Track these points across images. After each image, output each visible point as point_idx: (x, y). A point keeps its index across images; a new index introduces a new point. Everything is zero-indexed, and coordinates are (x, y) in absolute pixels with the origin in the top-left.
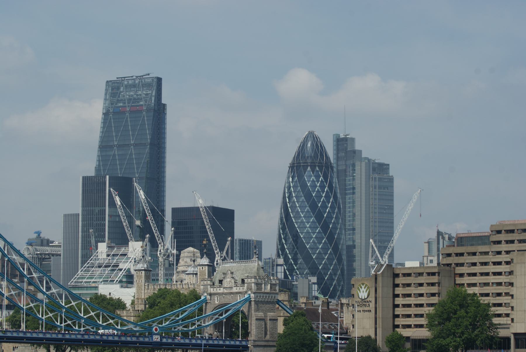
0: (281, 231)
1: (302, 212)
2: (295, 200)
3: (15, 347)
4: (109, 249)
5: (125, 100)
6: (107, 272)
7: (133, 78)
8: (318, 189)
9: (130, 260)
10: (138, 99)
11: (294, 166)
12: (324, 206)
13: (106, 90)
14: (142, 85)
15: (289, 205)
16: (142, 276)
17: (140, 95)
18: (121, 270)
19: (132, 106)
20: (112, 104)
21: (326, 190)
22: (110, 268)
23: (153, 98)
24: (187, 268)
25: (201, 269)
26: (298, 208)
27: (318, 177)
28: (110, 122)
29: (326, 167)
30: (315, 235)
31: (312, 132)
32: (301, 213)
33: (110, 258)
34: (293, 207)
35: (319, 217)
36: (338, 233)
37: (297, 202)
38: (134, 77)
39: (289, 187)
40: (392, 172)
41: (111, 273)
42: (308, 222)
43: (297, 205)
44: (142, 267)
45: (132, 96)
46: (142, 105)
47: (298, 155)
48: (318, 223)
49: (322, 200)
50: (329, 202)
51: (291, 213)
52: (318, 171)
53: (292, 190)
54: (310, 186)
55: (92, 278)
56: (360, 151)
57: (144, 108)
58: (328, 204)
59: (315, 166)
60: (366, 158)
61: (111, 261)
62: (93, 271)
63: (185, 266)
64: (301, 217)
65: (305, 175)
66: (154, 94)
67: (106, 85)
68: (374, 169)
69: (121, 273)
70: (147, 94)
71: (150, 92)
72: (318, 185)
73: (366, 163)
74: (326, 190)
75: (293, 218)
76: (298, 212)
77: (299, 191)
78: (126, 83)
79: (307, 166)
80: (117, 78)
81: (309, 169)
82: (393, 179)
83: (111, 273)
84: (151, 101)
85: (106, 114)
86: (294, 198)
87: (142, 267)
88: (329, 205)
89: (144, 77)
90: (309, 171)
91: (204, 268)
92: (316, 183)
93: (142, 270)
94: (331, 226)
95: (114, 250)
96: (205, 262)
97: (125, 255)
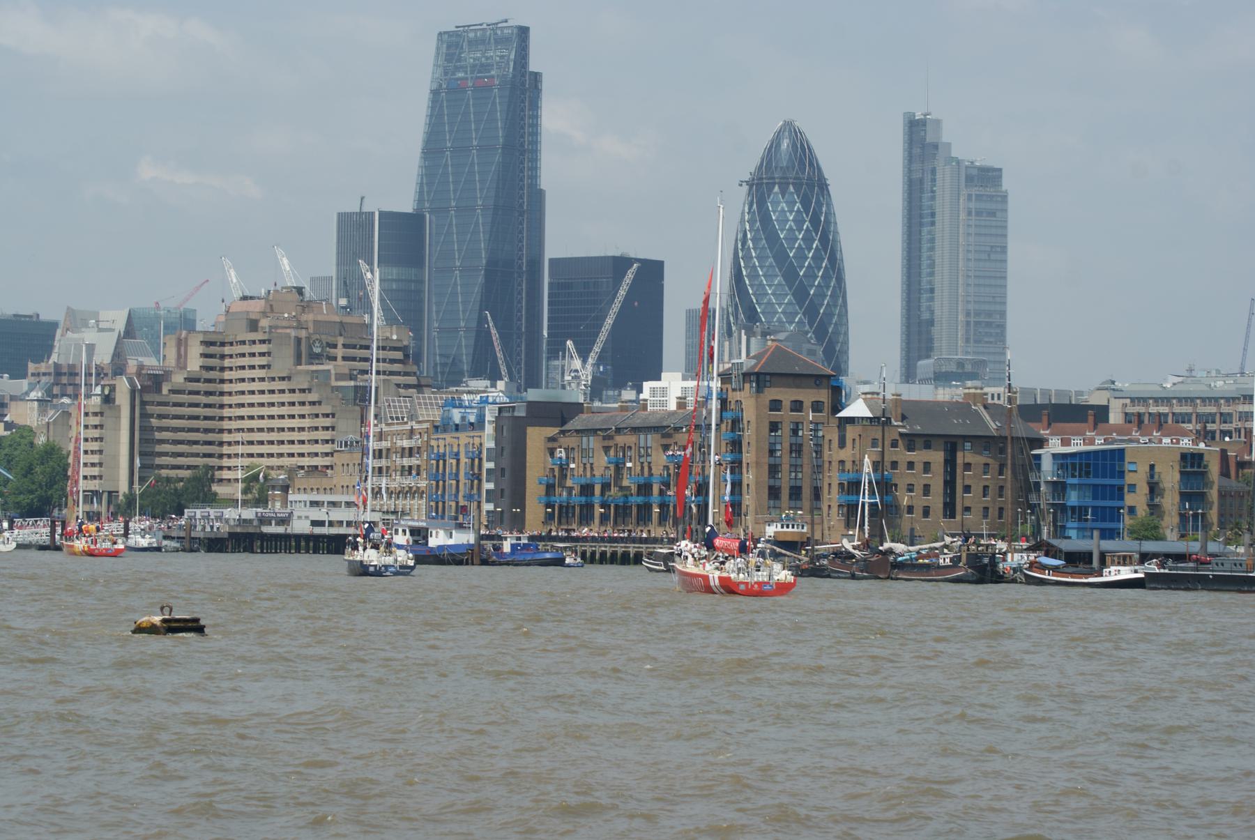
0: (732, 319)
1: (770, 286)
2: (757, 264)
8: (800, 244)
12: (811, 275)
15: (744, 273)
21: (814, 246)
32: (767, 288)
34: (754, 276)
35: (800, 294)
37: (761, 267)
43: (761, 273)
49: (806, 264)
50: (819, 268)
53: (751, 245)
71: (505, 53)
72: (801, 236)
76: (761, 285)
77: (763, 248)
86: (755, 260)
88: (820, 274)
89: (500, 25)
92: (797, 233)
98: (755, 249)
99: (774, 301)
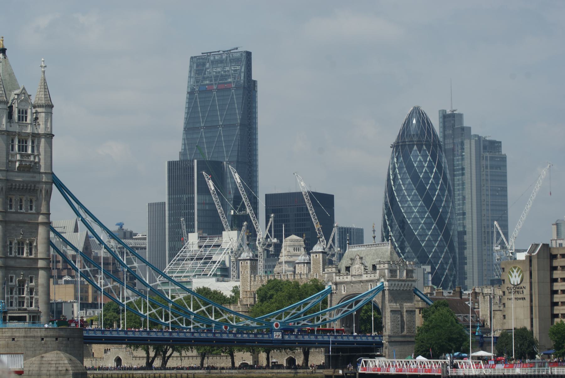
0: (386, 217)
1: (409, 196)
2: (401, 183)
3: (106, 349)
4: (200, 240)
5: (211, 77)
6: (199, 265)
7: (220, 53)
8: (426, 170)
9: (224, 251)
10: (226, 75)
11: (399, 145)
12: (433, 189)
13: (191, 67)
14: (230, 60)
15: (394, 189)
16: (247, 266)
17: (228, 71)
18: (214, 262)
19: (219, 84)
20: (197, 82)
21: (434, 171)
22: (202, 261)
23: (242, 75)
24: (290, 258)
25: (315, 257)
26: (405, 191)
27: (425, 156)
28: (196, 102)
29: (433, 145)
30: (423, 221)
31: (417, 108)
33: (202, 249)
34: (399, 190)
35: (427, 200)
36: (449, 218)
37: (404, 184)
38: (221, 52)
39: (394, 168)
40: (504, 151)
41: (203, 266)
42: (415, 207)
43: (403, 188)
44: (247, 257)
45: (219, 72)
46: (230, 83)
47: (403, 133)
48: (427, 208)
49: (430, 182)
50: (438, 184)
51: (396, 197)
52: (425, 150)
53: (398, 172)
54: (417, 166)
55: (182, 272)
56: (470, 128)
57: (233, 86)
58: (438, 186)
59: (422, 145)
61: (203, 253)
62: (184, 264)
63: (288, 256)
64: (408, 201)
65: (412, 155)
66: (243, 70)
67: (190, 61)
68: (485, 148)
69: (214, 266)
70: (235, 71)
71: (238, 68)
72: (426, 165)
73: (476, 140)
74: (434, 171)
75: (399, 203)
76: (404, 195)
77: (405, 173)
78: (212, 58)
79: (413, 145)
80: (203, 53)
81: (415, 147)
82: (506, 158)
83: (203, 266)
84: (241, 78)
85: (191, 93)
86: (400, 180)
87: (247, 257)
88: (439, 188)
89: (232, 51)
92: (424, 163)
94: (441, 210)
95: (206, 241)
96: (319, 249)
97: (219, 246)
98: (400, 174)
99: (412, 205)
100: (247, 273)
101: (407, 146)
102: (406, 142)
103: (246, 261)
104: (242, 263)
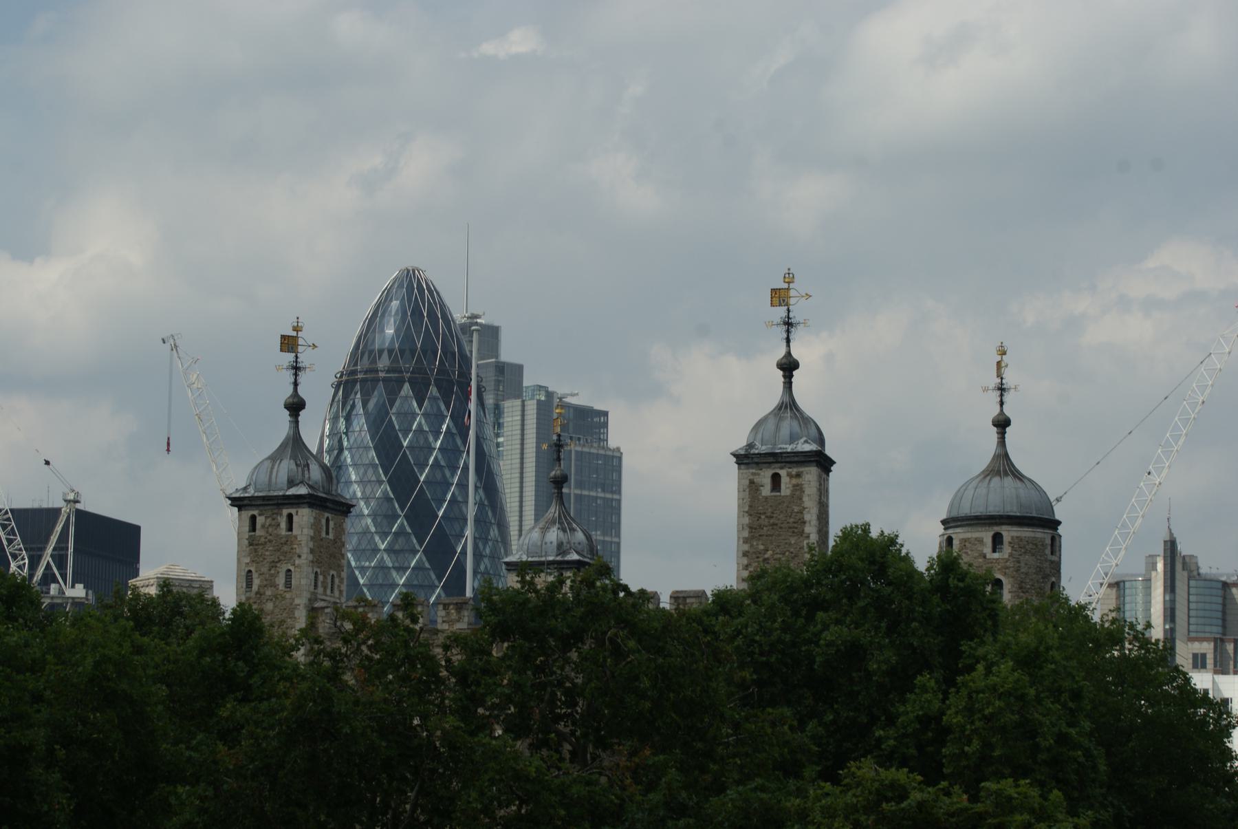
11: (355, 381)
16: (289, 541)
25: (766, 491)
27: (435, 419)
31: (408, 271)
42: (401, 569)
44: (291, 483)
52: (434, 399)
56: (518, 369)
60: (540, 386)
65: (394, 410)
73: (539, 402)
79: (400, 382)
81: (406, 389)
82: (620, 459)
87: (291, 483)
90: (407, 397)
91: (785, 480)
93: (297, 501)
96: (793, 438)
100: (288, 584)
101: (381, 382)
102: (377, 371)
103: (285, 512)
104: (260, 520)
